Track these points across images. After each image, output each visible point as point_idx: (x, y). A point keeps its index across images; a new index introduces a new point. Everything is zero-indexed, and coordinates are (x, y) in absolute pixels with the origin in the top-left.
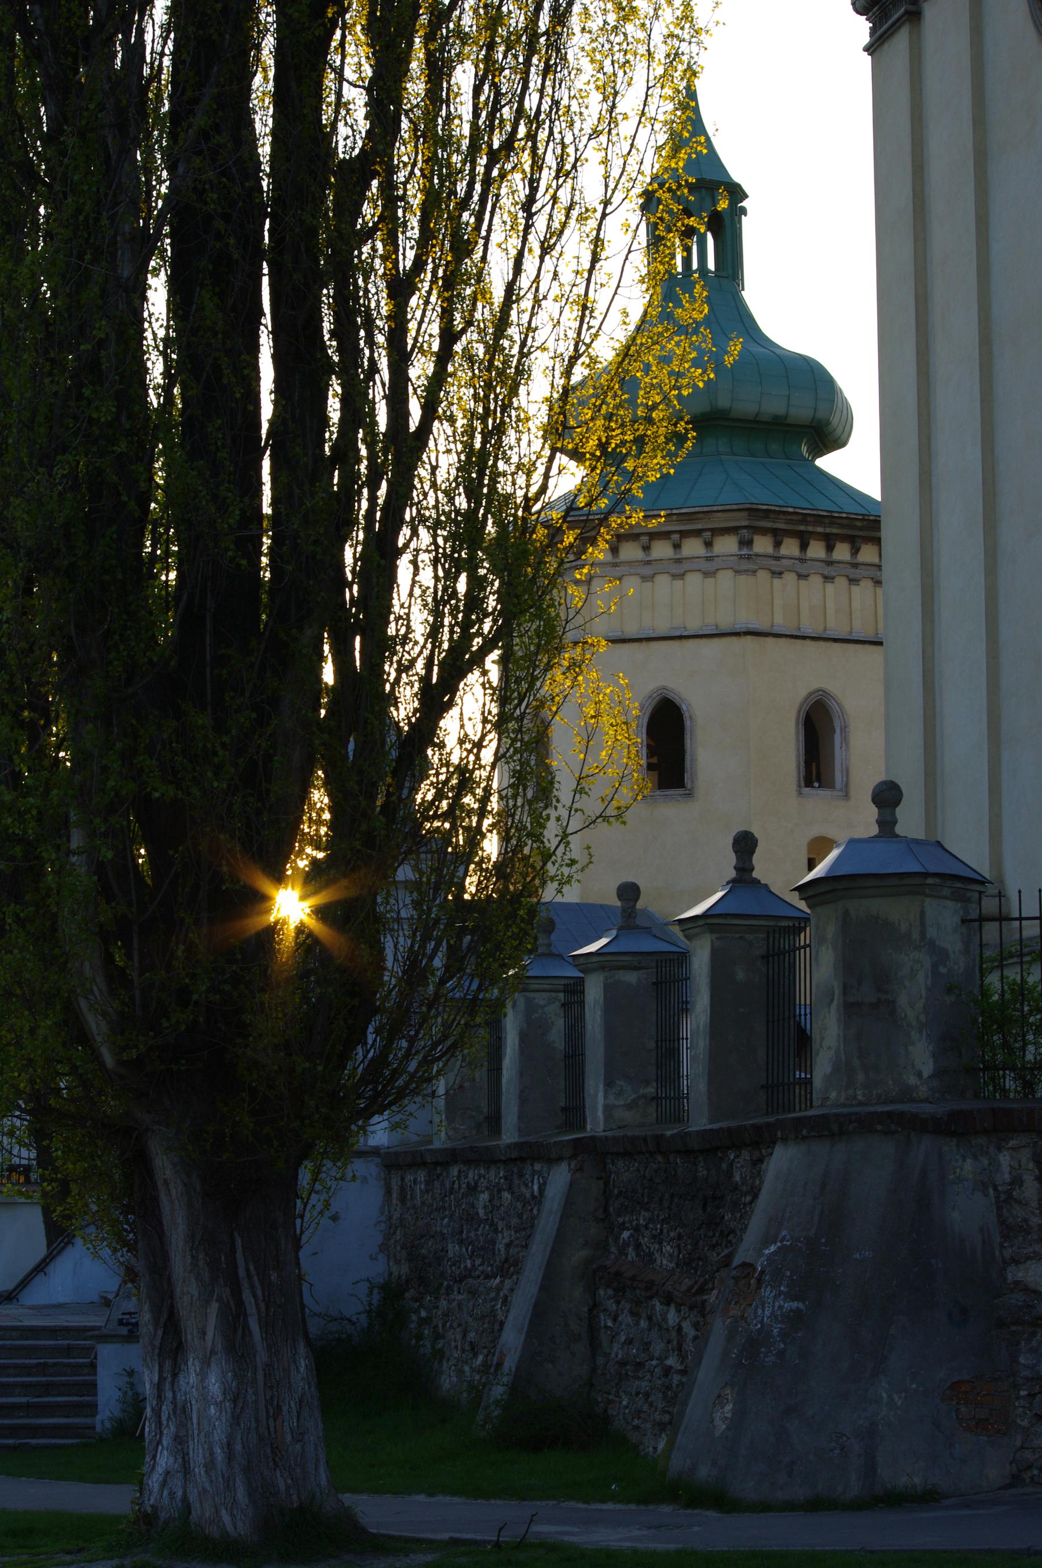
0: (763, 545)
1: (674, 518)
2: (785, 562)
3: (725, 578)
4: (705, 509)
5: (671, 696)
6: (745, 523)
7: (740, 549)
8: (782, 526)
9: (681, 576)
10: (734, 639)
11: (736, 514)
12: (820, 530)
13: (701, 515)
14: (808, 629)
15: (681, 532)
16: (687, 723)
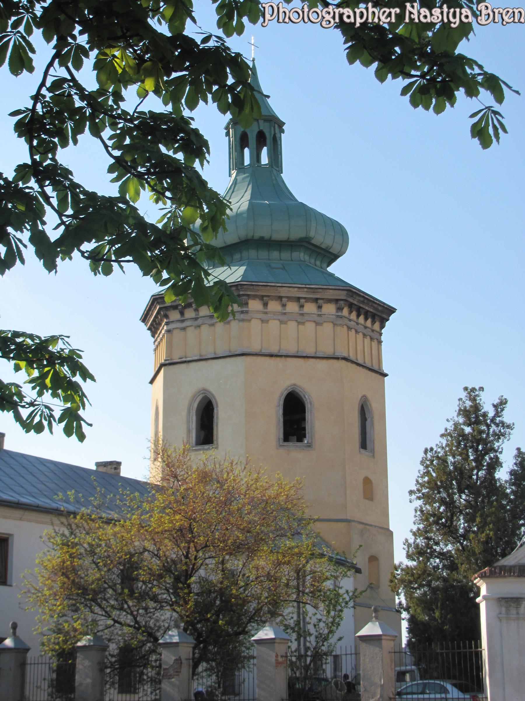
0: (345, 312)
1: (306, 290)
2: (352, 323)
3: (328, 328)
4: (325, 287)
5: (298, 390)
6: (344, 298)
7: (337, 312)
8: (356, 303)
9: (303, 323)
10: (335, 361)
11: (340, 292)
12: (367, 308)
13: (321, 290)
14: (360, 361)
15: (305, 298)
16: (308, 406)
